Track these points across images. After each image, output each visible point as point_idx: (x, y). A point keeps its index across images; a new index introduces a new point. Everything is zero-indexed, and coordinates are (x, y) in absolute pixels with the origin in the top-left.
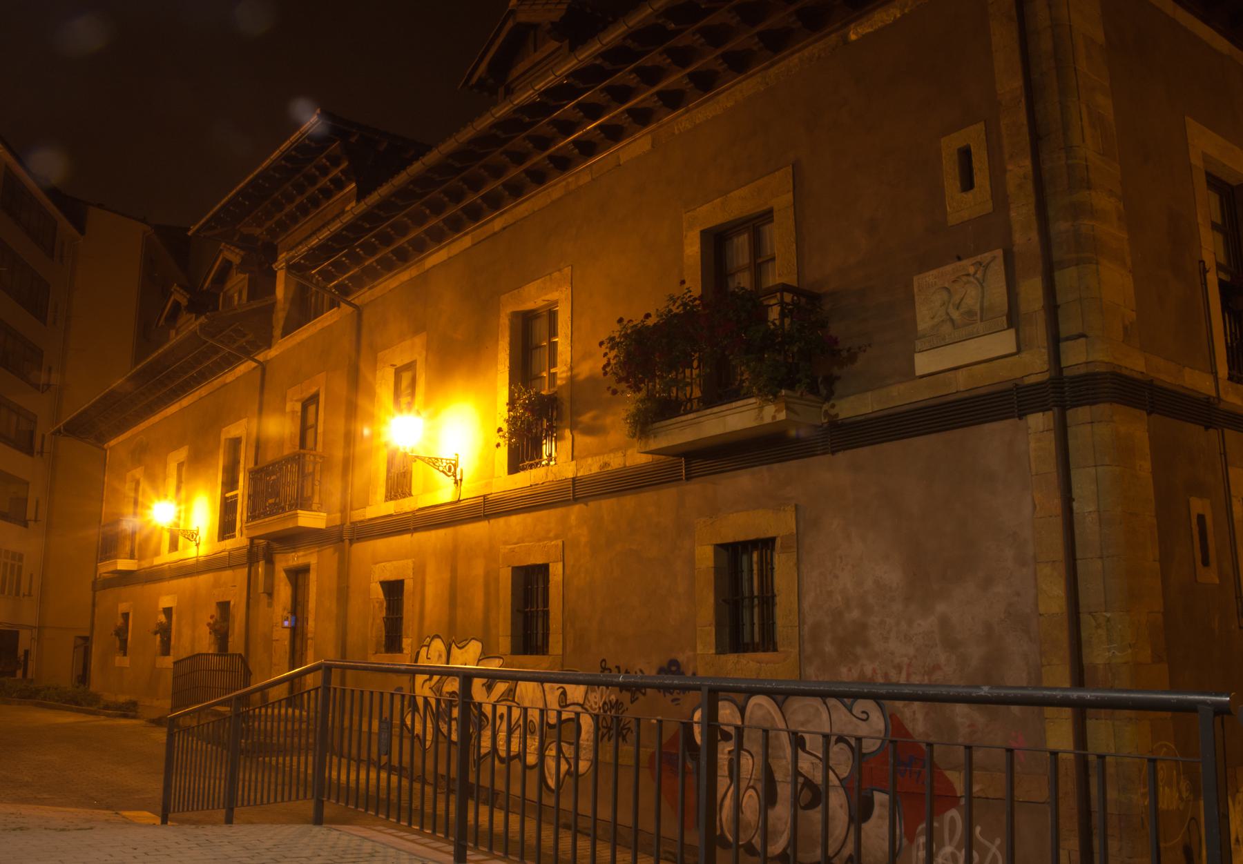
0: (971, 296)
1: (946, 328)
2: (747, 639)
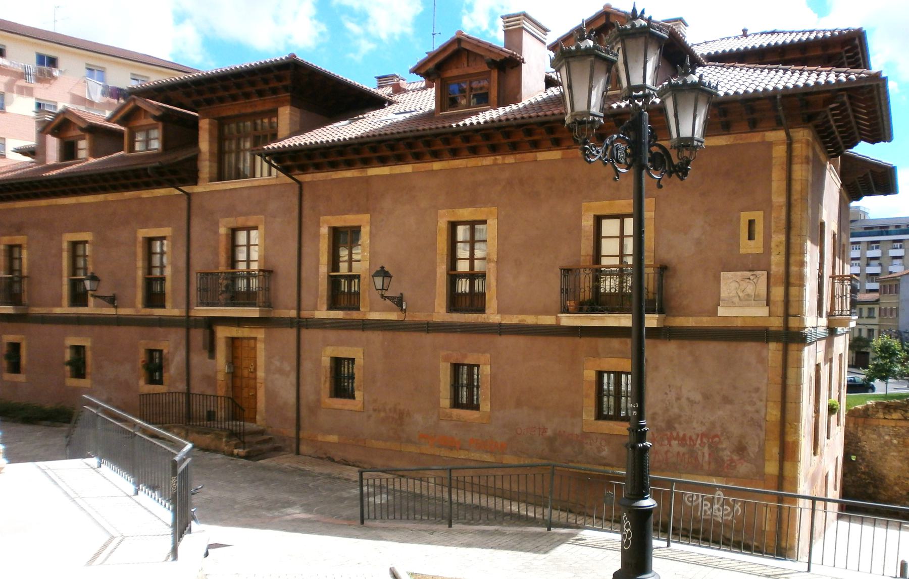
0: (750, 289)
1: (736, 300)
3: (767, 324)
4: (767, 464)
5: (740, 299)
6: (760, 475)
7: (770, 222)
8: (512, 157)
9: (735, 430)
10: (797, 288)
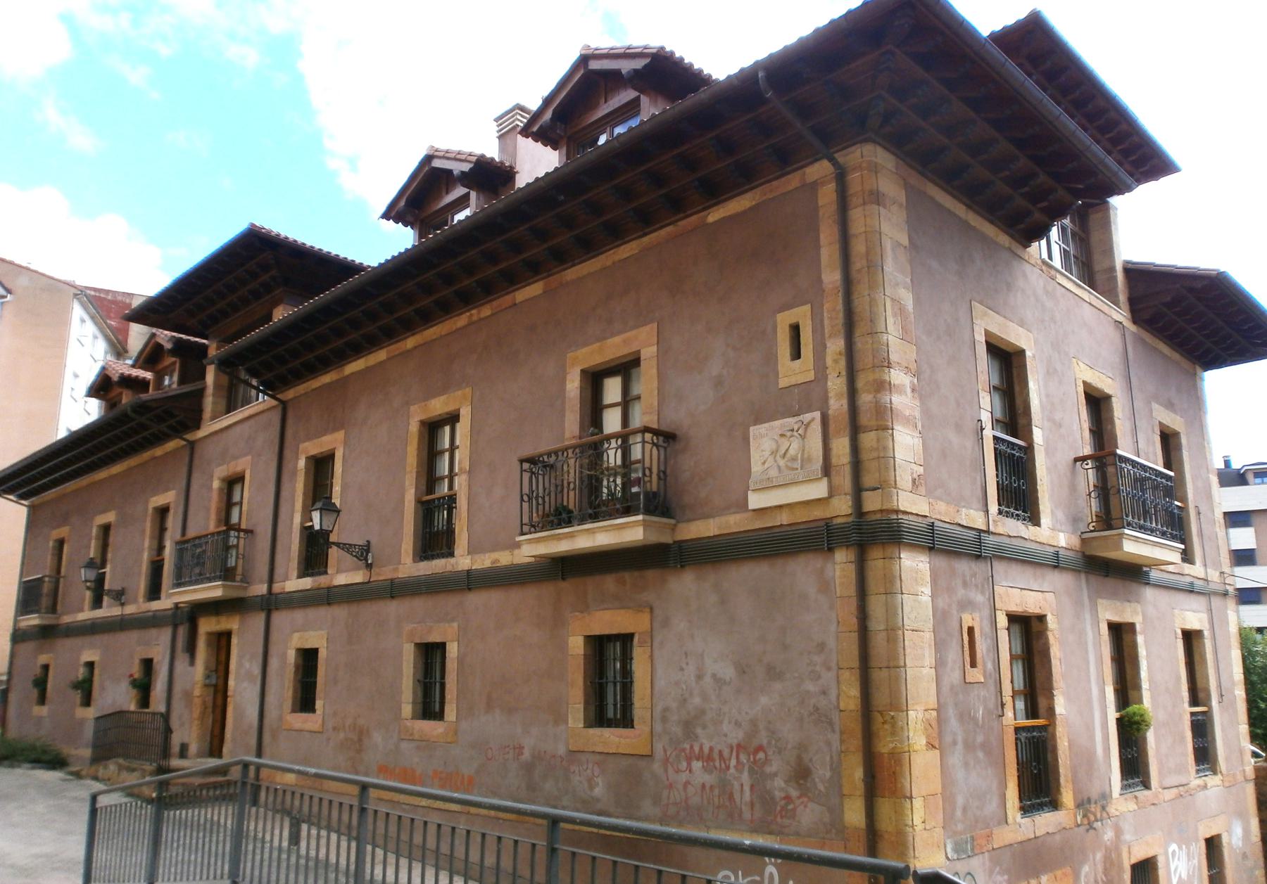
2: (610, 714)
3: (828, 514)
4: (848, 804)
5: (780, 472)
6: (836, 827)
7: (822, 321)
8: (488, 306)
9: (789, 733)
10: (873, 434)
